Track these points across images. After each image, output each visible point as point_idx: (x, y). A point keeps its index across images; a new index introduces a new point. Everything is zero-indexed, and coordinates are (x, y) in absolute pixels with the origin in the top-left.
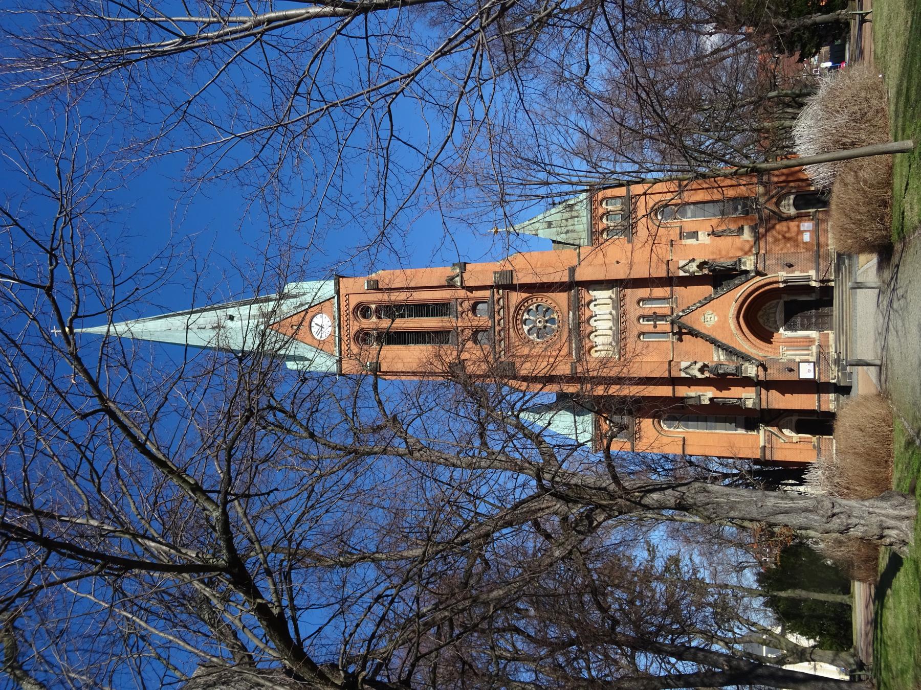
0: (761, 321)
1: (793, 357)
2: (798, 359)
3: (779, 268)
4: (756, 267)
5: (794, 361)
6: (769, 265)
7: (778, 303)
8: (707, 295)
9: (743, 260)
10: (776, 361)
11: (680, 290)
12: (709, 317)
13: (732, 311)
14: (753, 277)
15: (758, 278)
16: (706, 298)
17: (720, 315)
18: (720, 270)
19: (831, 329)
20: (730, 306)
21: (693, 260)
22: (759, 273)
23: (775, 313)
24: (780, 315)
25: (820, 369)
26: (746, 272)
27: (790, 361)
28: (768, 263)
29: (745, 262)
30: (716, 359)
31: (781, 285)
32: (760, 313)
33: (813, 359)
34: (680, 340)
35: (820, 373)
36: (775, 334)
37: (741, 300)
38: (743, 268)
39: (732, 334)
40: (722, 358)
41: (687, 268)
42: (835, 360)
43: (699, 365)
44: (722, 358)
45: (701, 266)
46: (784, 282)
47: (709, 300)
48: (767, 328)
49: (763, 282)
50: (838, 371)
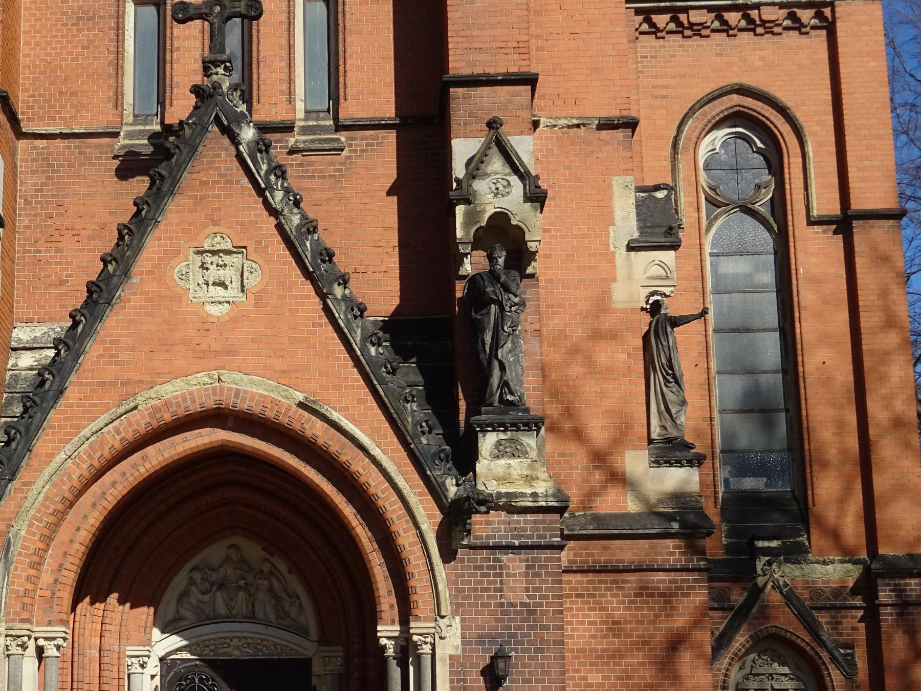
0: (214, 553)
3: (486, 621)
4: (488, 503)
6: (499, 570)
7: (303, 632)
8: (342, 263)
9: (529, 441)
11: (381, 159)
12: (229, 274)
13: (254, 388)
14: (435, 491)
15: (429, 517)
16: (328, 255)
17: (240, 326)
18: (477, 329)
20: (282, 376)
22: (456, 517)
23: (251, 617)
24: (244, 639)
26: (464, 458)
28: (514, 564)
29: (517, 452)
30: (22, 334)
31: (387, 631)
34: (129, 165)
36: (145, 613)
37: (316, 430)
38: (488, 442)
39: (131, 387)
40: (26, 360)
41: (496, 164)
45: (503, 235)
46: (407, 649)
47: (319, 270)
49: (406, 539)
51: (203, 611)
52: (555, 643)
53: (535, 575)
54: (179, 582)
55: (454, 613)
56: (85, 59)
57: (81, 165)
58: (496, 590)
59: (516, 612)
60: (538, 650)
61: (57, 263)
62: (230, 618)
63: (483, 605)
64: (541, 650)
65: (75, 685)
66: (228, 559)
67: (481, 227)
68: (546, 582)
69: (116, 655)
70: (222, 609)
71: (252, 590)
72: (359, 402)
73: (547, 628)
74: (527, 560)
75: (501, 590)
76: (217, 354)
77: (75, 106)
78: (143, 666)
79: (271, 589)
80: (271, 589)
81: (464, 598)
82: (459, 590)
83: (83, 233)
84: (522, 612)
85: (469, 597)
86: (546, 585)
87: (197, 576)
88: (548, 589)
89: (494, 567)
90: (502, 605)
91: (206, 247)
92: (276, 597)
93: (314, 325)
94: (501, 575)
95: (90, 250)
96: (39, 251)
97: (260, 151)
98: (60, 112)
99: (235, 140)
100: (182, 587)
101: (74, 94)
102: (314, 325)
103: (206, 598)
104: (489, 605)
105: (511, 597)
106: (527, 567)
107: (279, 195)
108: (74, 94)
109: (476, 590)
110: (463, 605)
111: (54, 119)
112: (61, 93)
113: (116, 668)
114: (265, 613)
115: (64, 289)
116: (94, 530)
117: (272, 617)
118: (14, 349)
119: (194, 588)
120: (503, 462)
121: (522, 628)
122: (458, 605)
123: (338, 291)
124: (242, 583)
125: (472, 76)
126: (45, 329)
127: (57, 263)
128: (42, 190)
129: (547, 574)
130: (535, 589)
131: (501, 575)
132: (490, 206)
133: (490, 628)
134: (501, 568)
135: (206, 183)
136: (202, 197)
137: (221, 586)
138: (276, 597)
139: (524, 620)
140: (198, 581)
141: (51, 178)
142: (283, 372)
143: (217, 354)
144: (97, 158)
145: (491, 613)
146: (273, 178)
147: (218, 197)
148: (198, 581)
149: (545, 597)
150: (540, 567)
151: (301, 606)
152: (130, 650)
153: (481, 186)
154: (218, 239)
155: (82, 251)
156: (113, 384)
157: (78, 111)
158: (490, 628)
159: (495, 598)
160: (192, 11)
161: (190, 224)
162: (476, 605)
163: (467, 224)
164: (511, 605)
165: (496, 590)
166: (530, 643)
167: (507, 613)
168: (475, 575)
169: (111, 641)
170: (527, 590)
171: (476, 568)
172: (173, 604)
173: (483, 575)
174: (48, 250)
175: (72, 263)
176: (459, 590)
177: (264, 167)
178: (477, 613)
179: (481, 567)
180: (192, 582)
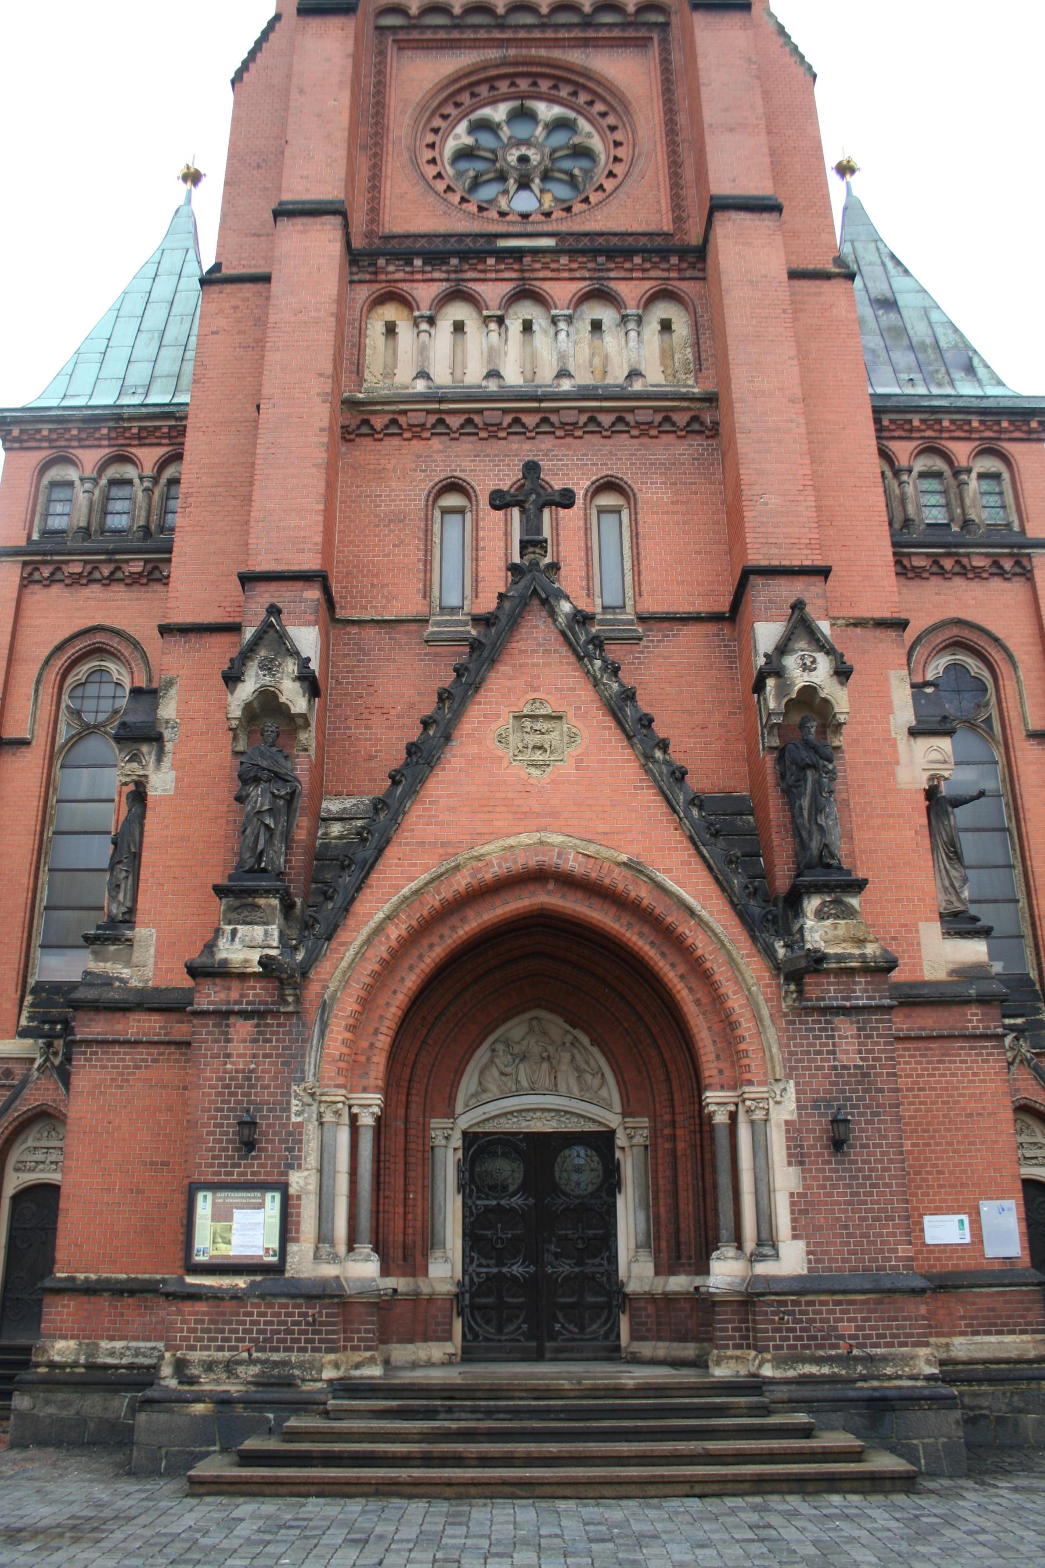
2: (302, 1181)
5: (294, 1163)
10: (292, 1067)
19: (468, 1356)
21: (843, 673)
25: (236, 1296)
27: (294, 1139)
28: (846, 1027)
30: (332, 806)
33: (303, 1263)
35: (214, 1296)
38: (812, 904)
42: (288, 1383)
43: (294, 696)
44: (336, 829)
48: (482, 1055)
50: (224, 1401)
52: (891, 1106)
53: (867, 1037)
55: (789, 1077)
56: (395, 555)
57: (390, 650)
58: (829, 1052)
59: (850, 1075)
60: (873, 1114)
61: (366, 740)
63: (817, 1068)
64: (878, 1114)
65: (382, 1157)
67: (791, 700)
68: (877, 1044)
69: (420, 1128)
72: (683, 863)
73: (881, 1091)
74: (858, 1022)
75: (834, 1052)
76: (538, 815)
77: (386, 597)
78: (447, 1138)
81: (797, 1061)
82: (791, 1053)
83: (392, 711)
84: (855, 1075)
85: (802, 1061)
86: (879, 1046)
88: (880, 1051)
89: (825, 1030)
90: (835, 1068)
91: (525, 712)
93: (636, 788)
94: (833, 1037)
95: (399, 728)
96: (350, 728)
97: (578, 622)
98: (371, 602)
99: (552, 614)
101: (384, 586)
102: (636, 788)
104: (822, 1068)
105: (844, 1059)
106: (859, 1029)
107: (598, 663)
108: (384, 586)
109: (808, 1053)
110: (796, 1068)
111: (366, 608)
112: (372, 585)
113: (420, 1141)
115: (373, 764)
116: (410, 993)
117: (576, 1091)
118: (324, 820)
121: (856, 1091)
122: (792, 1069)
123: (658, 754)
125: (770, 566)
126: (354, 801)
127: (366, 740)
128: (352, 672)
129: (879, 1036)
130: (868, 1052)
131: (833, 1037)
132: (799, 679)
133: (825, 1091)
134: (833, 1030)
135: (525, 651)
136: (521, 666)
139: (858, 1083)
141: (362, 661)
142: (605, 834)
143: (538, 815)
144: (406, 644)
145: (824, 1076)
146: (591, 647)
147: (537, 665)
149: (878, 1059)
150: (872, 1029)
152: (435, 1123)
153: (791, 662)
154: (538, 704)
155: (392, 728)
156: (433, 844)
157: (389, 601)
158: (825, 1091)
159: (829, 1060)
160: (508, 498)
162: (809, 1068)
163: (779, 696)
164: (845, 1067)
165: (829, 1052)
166: (865, 1106)
167: (841, 1076)
168: (807, 1038)
169: (415, 1112)
170: (860, 1052)
172: (475, 1079)
173: (815, 1037)
174: (357, 728)
175: (381, 740)
176: (791, 1053)
177: (583, 638)
178: (811, 1076)
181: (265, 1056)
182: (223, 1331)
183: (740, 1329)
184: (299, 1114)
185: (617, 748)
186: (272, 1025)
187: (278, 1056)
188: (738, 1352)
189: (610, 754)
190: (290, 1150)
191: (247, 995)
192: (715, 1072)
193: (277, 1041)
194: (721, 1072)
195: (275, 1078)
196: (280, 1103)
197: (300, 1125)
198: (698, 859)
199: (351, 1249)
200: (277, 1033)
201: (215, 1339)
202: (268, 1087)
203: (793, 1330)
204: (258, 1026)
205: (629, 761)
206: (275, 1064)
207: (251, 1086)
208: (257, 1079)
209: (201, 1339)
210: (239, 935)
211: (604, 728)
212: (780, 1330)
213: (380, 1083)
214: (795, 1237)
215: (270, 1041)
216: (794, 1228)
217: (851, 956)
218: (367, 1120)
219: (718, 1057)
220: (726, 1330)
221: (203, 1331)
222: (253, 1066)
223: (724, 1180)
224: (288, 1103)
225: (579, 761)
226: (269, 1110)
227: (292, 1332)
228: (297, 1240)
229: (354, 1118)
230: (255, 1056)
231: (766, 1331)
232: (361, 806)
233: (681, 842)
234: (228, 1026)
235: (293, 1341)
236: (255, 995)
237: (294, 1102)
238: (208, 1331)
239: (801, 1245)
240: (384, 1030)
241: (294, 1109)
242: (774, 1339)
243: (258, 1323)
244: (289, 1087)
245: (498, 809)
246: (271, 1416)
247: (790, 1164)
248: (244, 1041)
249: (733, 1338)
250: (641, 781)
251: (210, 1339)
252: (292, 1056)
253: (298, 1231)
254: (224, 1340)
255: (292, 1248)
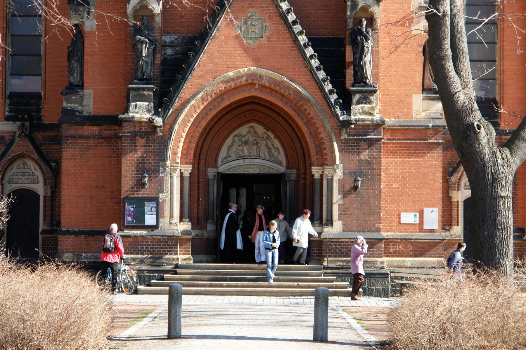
0: (243, 130)
1: (167, 188)
5: (162, 191)
7: (280, 163)
23: (259, 157)
32: (260, 129)
44: (169, 51)
51: (238, 153)
54: (229, 141)
62: (250, 157)
66: (249, 132)
68: (375, 152)
70: (247, 153)
71: (259, 145)
79: (267, 144)
80: (267, 144)
87: (236, 139)
92: (269, 148)
94: (359, 149)
100: (230, 143)
103: (240, 148)
114: (264, 155)
119: (235, 144)
120: (360, 106)
124: (255, 142)
126: (176, 37)
130: (372, 155)
131: (359, 149)
134: (359, 146)
137: (246, 143)
138: (269, 148)
140: (237, 141)
148: (237, 141)
151: (279, 152)
161: (242, 7)
164: (363, 160)
170: (368, 155)
171: (349, 146)
173: (352, 149)
179: (352, 146)
180: (234, 142)
181: (150, 152)
182: (138, 248)
183: (319, 250)
184: (162, 173)
185: (284, 33)
186: (152, 140)
187: (154, 152)
188: (318, 258)
189: (281, 35)
190: (160, 186)
191: (142, 129)
192: (315, 160)
193: (154, 146)
194: (317, 159)
195: (153, 160)
196: (156, 169)
197: (163, 177)
198: (313, 79)
199: (181, 220)
200: (154, 143)
201: (136, 250)
202: (151, 163)
203: (336, 251)
204: (146, 140)
205: (288, 38)
206: (154, 155)
207: (145, 163)
208: (147, 160)
209: (131, 251)
210: (138, 106)
211: (279, 24)
212: (331, 250)
213: (192, 161)
214: (339, 220)
215: (151, 146)
216: (339, 217)
217: (368, 120)
218: (187, 174)
219: (317, 154)
220: (314, 250)
221: (131, 248)
222: (145, 155)
223: (317, 199)
224: (159, 169)
225: (269, 38)
226: (152, 171)
227: (163, 248)
228: (163, 217)
229: (182, 174)
230: (146, 152)
231: (326, 250)
232: (179, 40)
233: (307, 72)
234: (135, 140)
235: (163, 251)
236: (145, 129)
237: (161, 168)
238: (133, 248)
239: (341, 222)
240: (192, 141)
241: (161, 171)
242: (329, 253)
243: (150, 245)
244: (159, 163)
245: (237, 58)
246: (157, 275)
247: (339, 194)
248: (142, 146)
249: (316, 253)
250: (293, 47)
251: (134, 251)
252: (159, 152)
253: (163, 214)
254: (139, 251)
255: (161, 220)
